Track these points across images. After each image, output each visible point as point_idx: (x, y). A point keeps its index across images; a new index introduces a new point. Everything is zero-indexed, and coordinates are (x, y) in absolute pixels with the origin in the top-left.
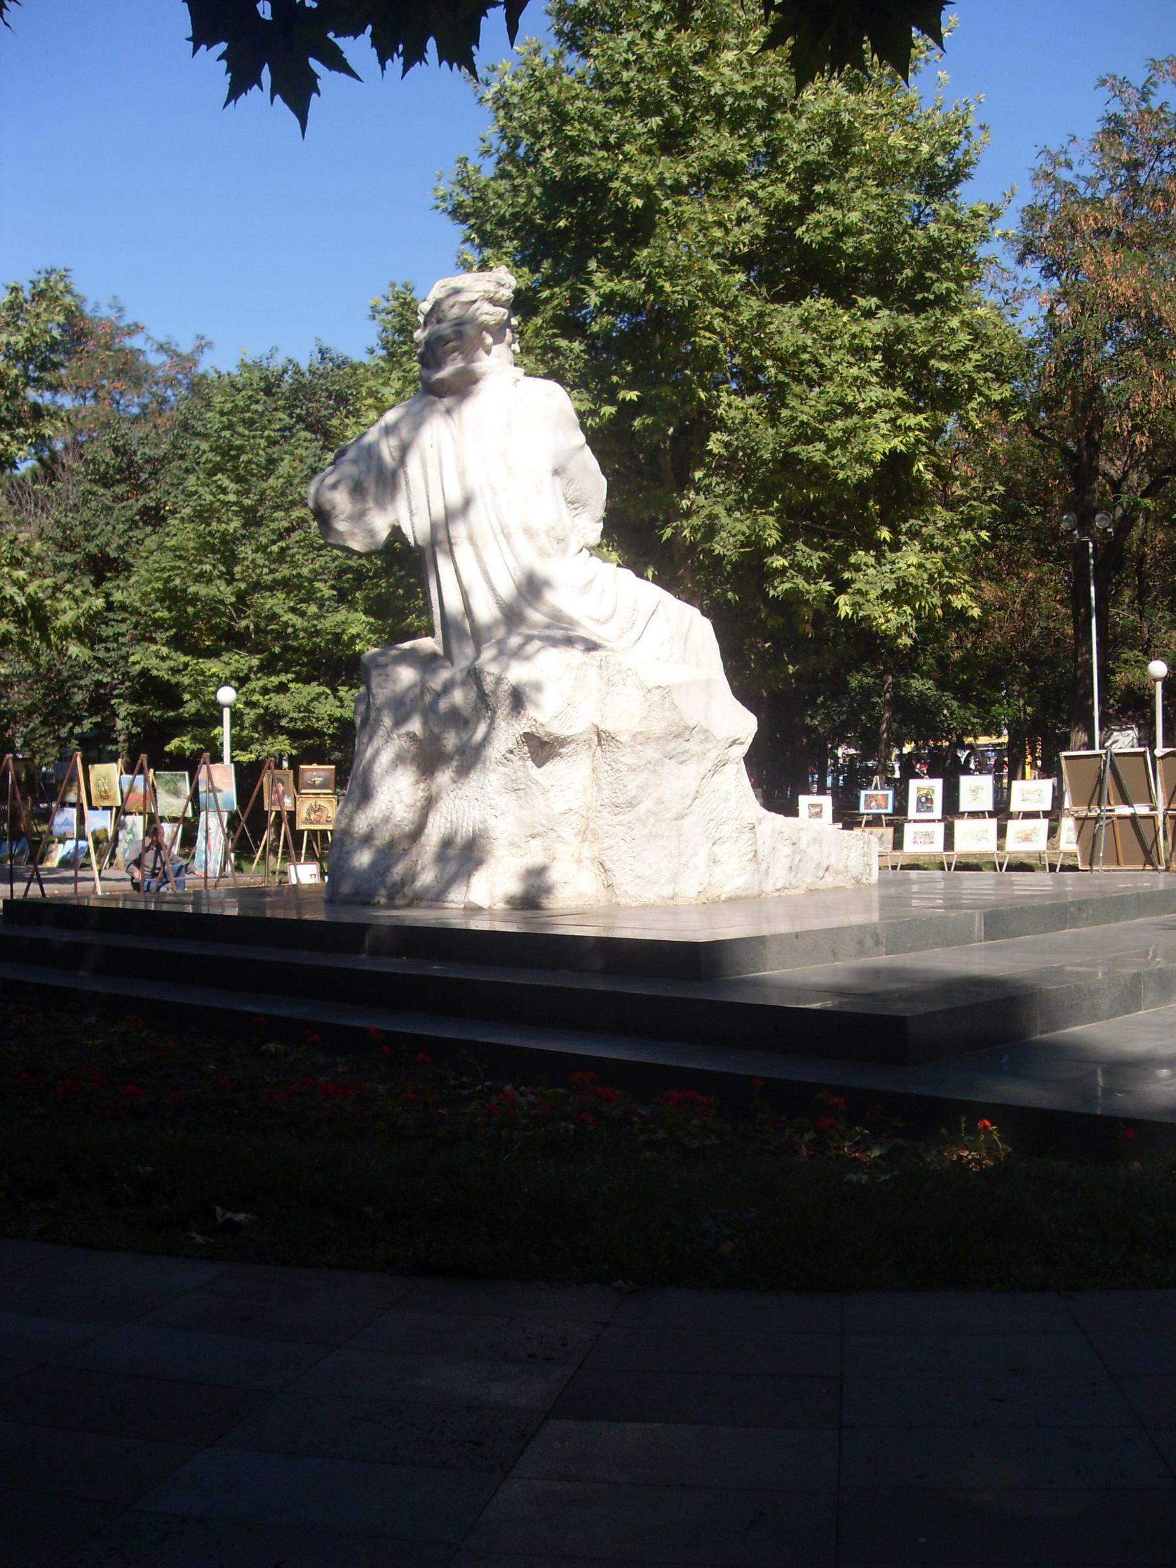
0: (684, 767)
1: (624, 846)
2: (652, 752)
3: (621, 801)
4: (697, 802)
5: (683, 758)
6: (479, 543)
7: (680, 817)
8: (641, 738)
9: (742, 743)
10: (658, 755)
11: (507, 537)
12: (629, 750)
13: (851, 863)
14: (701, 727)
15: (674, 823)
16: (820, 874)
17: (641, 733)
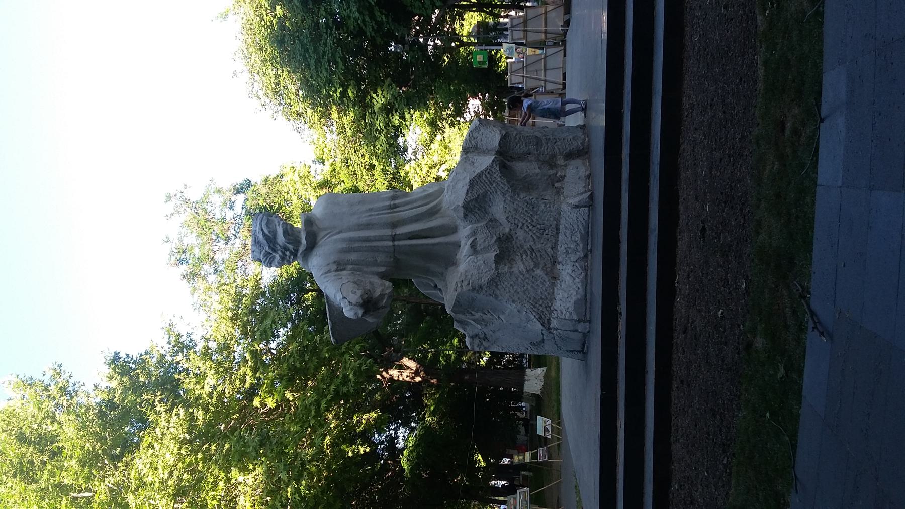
11: (395, 206)
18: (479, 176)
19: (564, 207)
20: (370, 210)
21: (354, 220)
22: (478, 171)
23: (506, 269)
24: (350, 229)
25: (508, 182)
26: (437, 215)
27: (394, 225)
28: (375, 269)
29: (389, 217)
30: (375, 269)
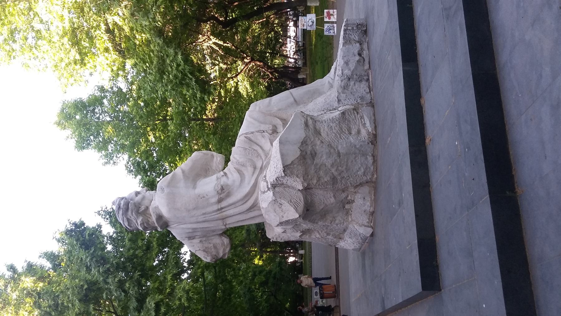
0: (318, 152)
2: (312, 171)
4: (333, 145)
5: (313, 153)
7: (339, 154)
9: (307, 120)
10: (313, 167)
11: (222, 208)
12: (310, 182)
13: (357, 38)
14: (300, 146)
15: (341, 157)
16: (362, 61)
19: (350, 226)
21: (194, 220)
25: (309, 221)
26: (255, 208)
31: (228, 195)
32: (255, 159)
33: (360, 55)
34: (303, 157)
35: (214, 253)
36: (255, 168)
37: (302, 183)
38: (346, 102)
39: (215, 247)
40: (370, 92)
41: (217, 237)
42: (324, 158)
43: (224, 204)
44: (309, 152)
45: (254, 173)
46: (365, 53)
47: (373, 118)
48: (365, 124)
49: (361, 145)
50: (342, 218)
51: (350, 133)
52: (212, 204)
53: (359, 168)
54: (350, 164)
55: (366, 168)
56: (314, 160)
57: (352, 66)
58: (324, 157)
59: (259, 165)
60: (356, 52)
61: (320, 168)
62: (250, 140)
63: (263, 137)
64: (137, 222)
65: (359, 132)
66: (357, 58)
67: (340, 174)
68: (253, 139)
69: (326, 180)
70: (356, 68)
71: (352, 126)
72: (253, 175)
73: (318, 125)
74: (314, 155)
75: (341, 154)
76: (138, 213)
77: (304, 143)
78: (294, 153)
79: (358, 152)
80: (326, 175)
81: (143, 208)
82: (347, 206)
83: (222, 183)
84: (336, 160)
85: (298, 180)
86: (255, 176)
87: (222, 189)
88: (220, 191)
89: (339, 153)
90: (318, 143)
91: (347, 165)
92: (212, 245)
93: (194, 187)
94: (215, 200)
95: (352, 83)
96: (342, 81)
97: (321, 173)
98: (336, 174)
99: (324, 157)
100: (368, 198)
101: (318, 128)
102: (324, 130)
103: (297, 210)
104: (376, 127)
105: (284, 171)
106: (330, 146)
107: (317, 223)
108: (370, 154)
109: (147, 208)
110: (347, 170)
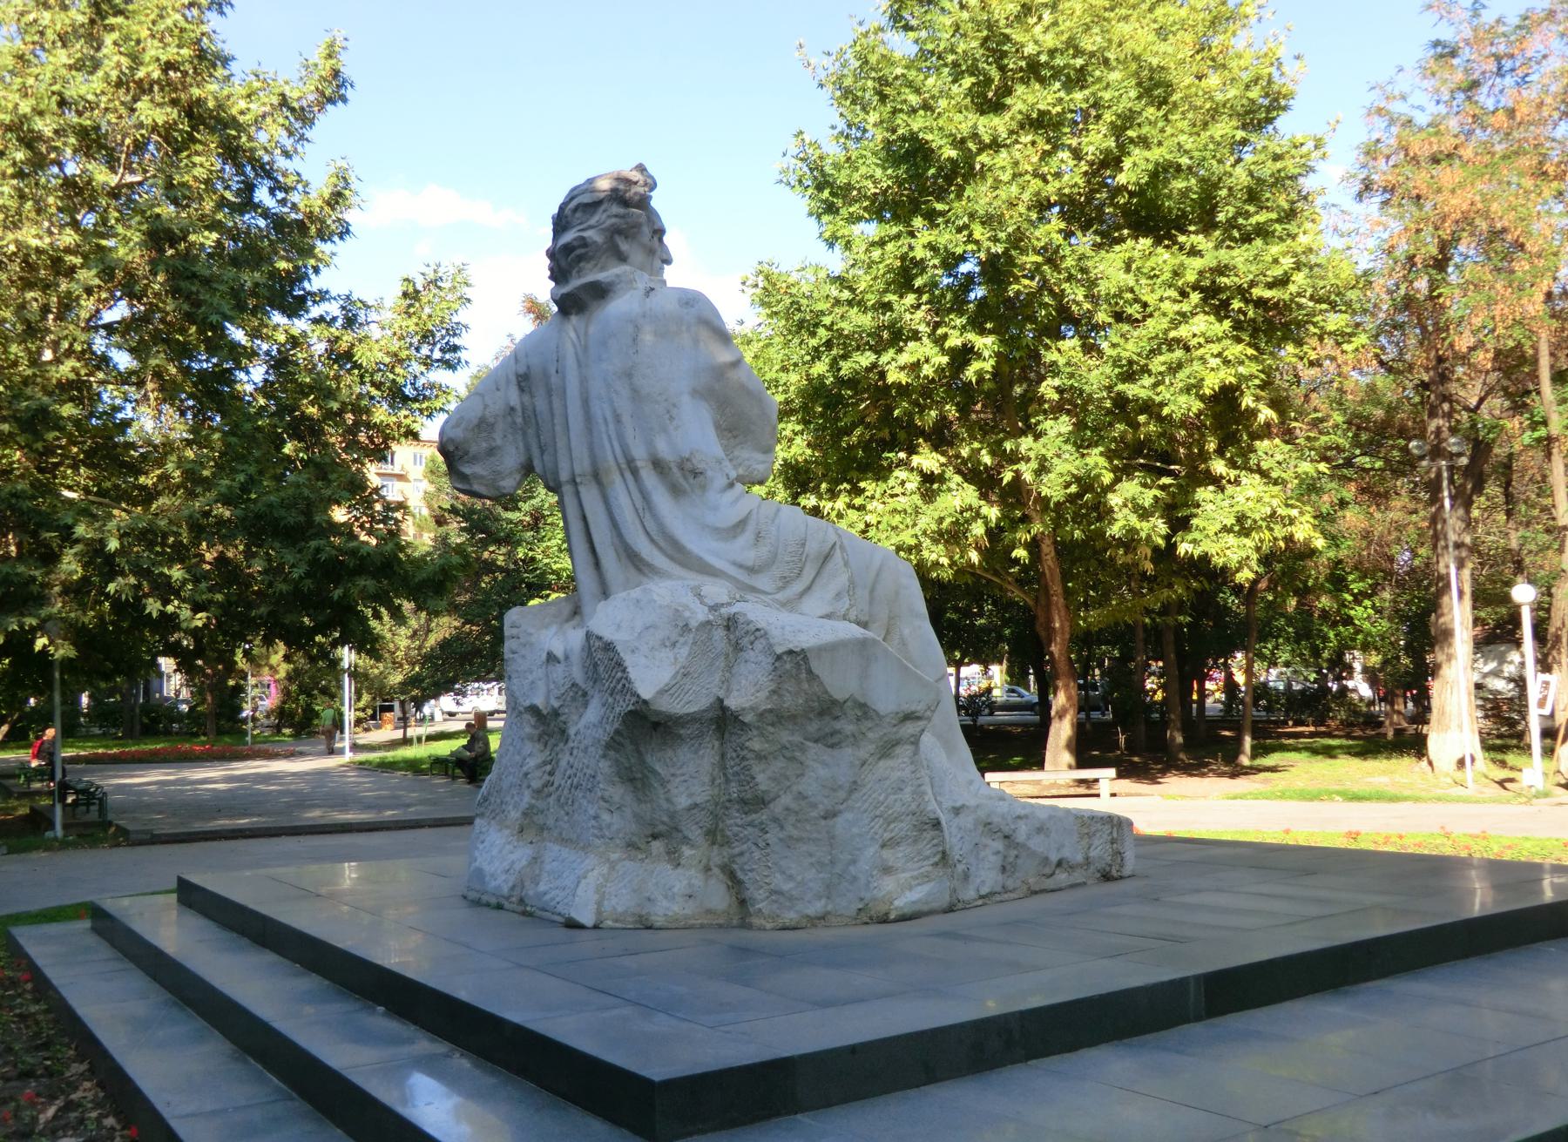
0: (836, 752)
1: (757, 855)
2: (785, 736)
3: (749, 796)
4: (856, 795)
5: (835, 740)
6: (605, 480)
7: (830, 815)
8: (770, 718)
9: (919, 718)
10: (797, 738)
11: (635, 472)
12: (755, 732)
15: (823, 822)
16: (1048, 871)
17: (771, 711)
18: (620, 665)
19: (591, 860)
20: (618, 419)
21: (597, 387)
22: (628, 660)
23: (528, 730)
24: (583, 381)
25: (617, 732)
26: (632, 570)
27: (597, 476)
28: (536, 452)
29: (610, 457)
30: (536, 452)
31: (676, 491)
32: (776, 571)
33: (1059, 864)
34: (828, 708)
35: (474, 449)
36: (752, 570)
37: (752, 708)
38: (954, 830)
39: (491, 452)
40: (982, 897)
41: (522, 459)
42: (823, 769)
43: (650, 478)
44: (838, 725)
45: (741, 566)
46: (1062, 877)
47: (925, 908)
48: (911, 888)
49: (855, 878)
50: (618, 831)
51: (883, 846)
52: (650, 444)
53: (791, 877)
54: (804, 848)
55: (791, 898)
56: (816, 741)
57: (1038, 844)
58: (823, 772)
59: (763, 582)
60: (1066, 853)
61: (792, 759)
62: (827, 558)
63: (838, 596)
64: (591, 227)
65: (887, 870)
66: (1054, 858)
67: (775, 820)
68: (830, 566)
69: (760, 778)
70: (1033, 854)
71: (903, 850)
72: (734, 563)
73: (904, 751)
74: (831, 740)
75: (830, 822)
76: (615, 232)
77: (864, 711)
78: (840, 682)
79: (838, 870)
80: (774, 779)
81: (624, 246)
82: (657, 846)
83: (709, 473)
84: (814, 806)
85: (763, 695)
86: (733, 571)
87: (696, 474)
88: (688, 466)
89: (835, 815)
90: (862, 753)
91: (799, 840)
92: (499, 442)
93: (695, 393)
94: (663, 449)
95: (999, 845)
96: (1003, 817)
97: (779, 764)
98: (777, 808)
99: (823, 772)
100: (689, 908)
101: (898, 750)
102: (896, 767)
103: (662, 692)
104: (903, 918)
105: (791, 652)
106: (854, 787)
107: (604, 756)
108: (829, 908)
109: (622, 258)
110: (789, 842)
